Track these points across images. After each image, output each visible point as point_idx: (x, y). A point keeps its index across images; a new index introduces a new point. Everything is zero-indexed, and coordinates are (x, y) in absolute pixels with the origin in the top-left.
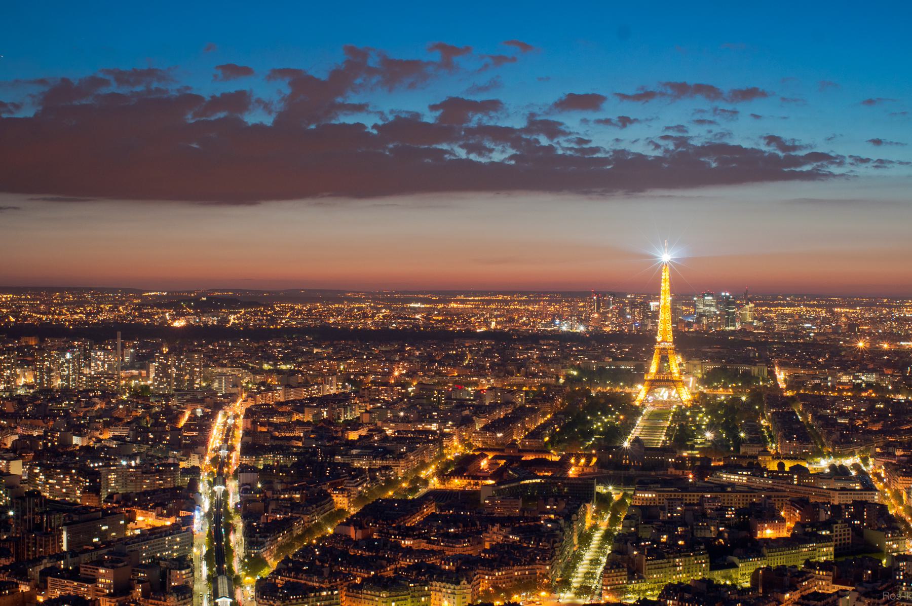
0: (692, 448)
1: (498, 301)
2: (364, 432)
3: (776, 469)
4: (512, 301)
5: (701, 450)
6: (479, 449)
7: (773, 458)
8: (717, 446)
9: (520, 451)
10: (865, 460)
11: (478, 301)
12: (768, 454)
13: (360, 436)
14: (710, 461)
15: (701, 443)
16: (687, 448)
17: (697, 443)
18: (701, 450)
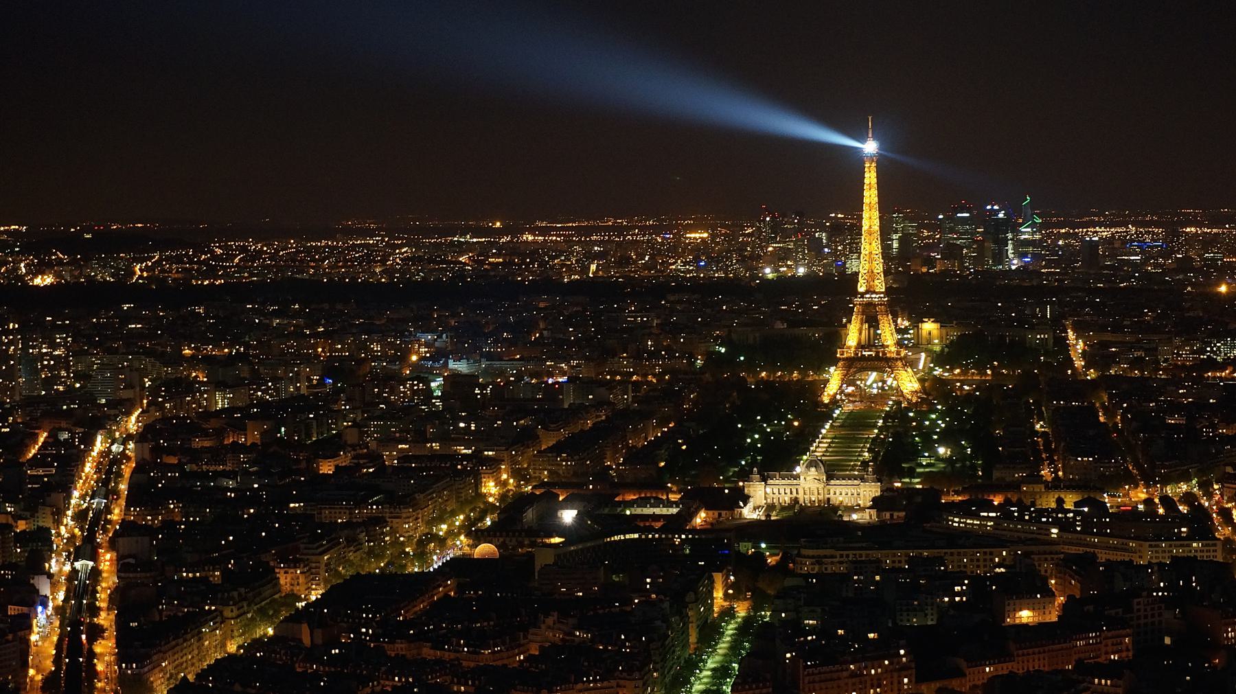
0: (911, 473)
1: (607, 229)
2: (344, 459)
3: (1053, 505)
4: (628, 229)
5: (926, 477)
6: (542, 484)
7: (1047, 487)
8: (953, 473)
9: (614, 485)
10: (1205, 486)
11: (571, 228)
12: (1039, 479)
13: (337, 467)
14: (939, 494)
15: (928, 465)
16: (901, 474)
17: (921, 466)
18: (926, 477)
